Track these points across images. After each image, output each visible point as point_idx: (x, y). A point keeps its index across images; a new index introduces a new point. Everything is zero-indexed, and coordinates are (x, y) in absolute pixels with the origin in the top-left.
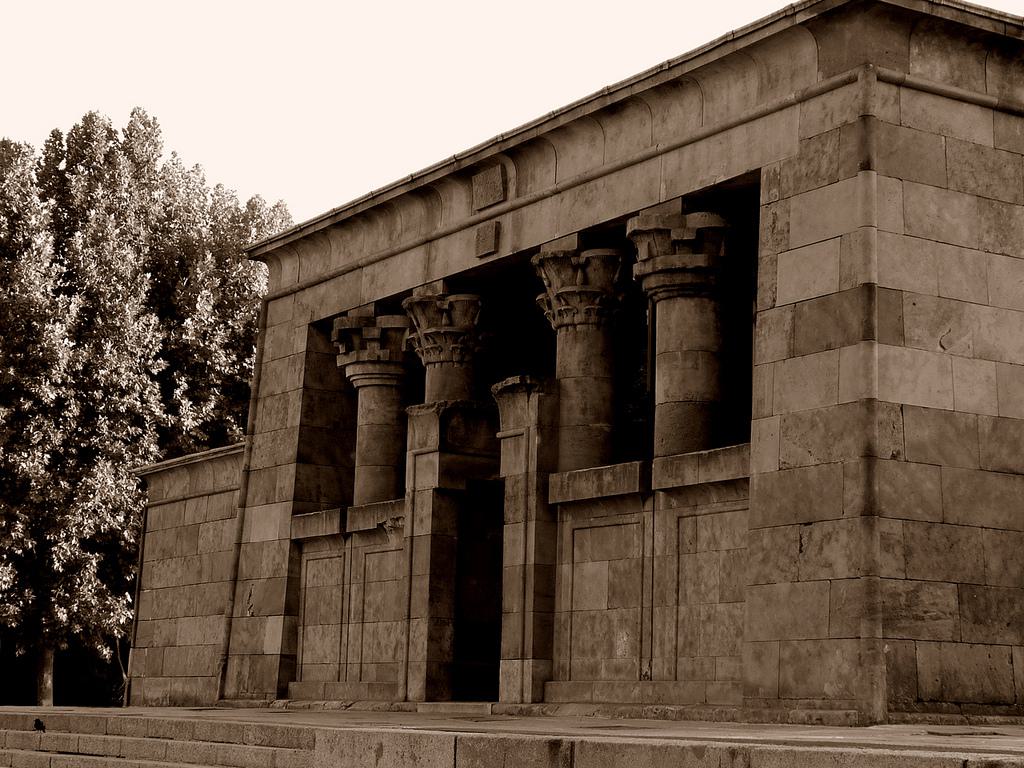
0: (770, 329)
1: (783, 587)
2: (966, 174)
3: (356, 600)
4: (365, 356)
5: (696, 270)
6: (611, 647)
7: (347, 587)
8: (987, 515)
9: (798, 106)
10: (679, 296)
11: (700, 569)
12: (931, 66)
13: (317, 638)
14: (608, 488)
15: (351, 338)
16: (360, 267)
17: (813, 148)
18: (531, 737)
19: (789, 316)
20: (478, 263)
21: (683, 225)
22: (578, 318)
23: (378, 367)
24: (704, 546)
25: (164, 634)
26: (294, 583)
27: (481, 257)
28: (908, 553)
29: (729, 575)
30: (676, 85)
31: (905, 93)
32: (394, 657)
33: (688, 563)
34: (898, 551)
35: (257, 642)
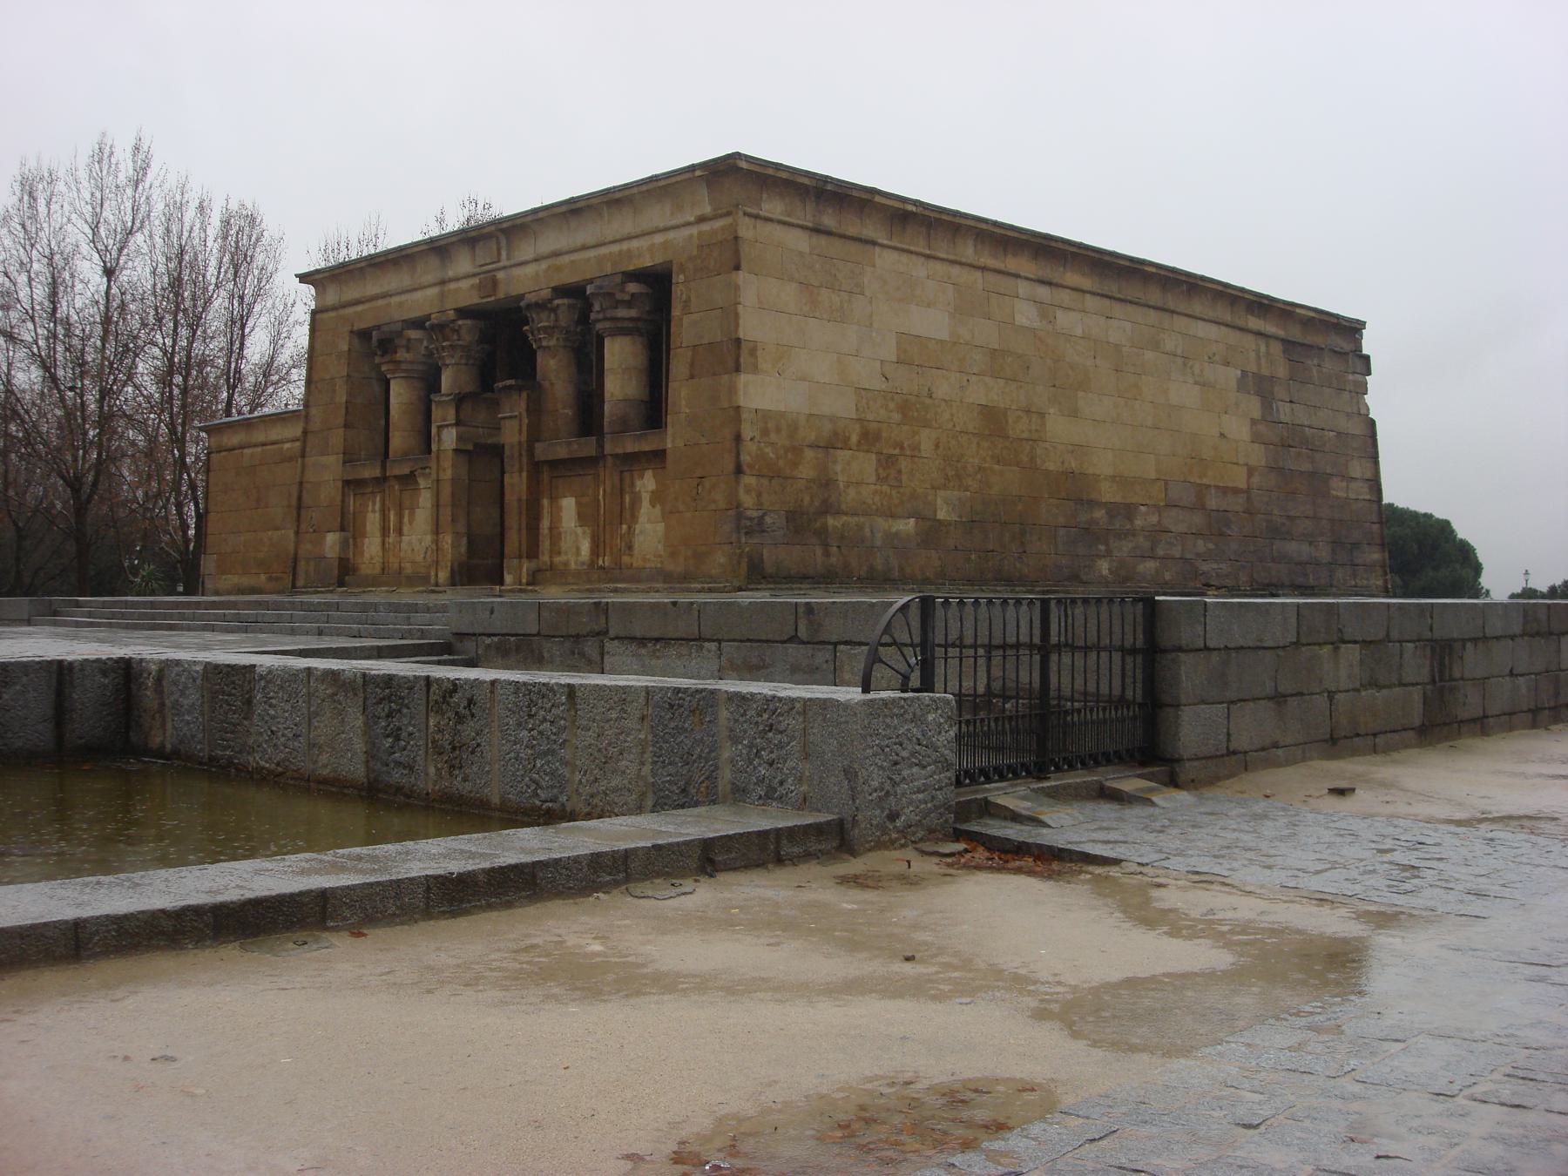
5: (631, 319)
6: (578, 549)
12: (773, 206)
19: (690, 353)
21: (623, 291)
28: (759, 495)
30: (618, 202)
31: (759, 223)
34: (754, 494)
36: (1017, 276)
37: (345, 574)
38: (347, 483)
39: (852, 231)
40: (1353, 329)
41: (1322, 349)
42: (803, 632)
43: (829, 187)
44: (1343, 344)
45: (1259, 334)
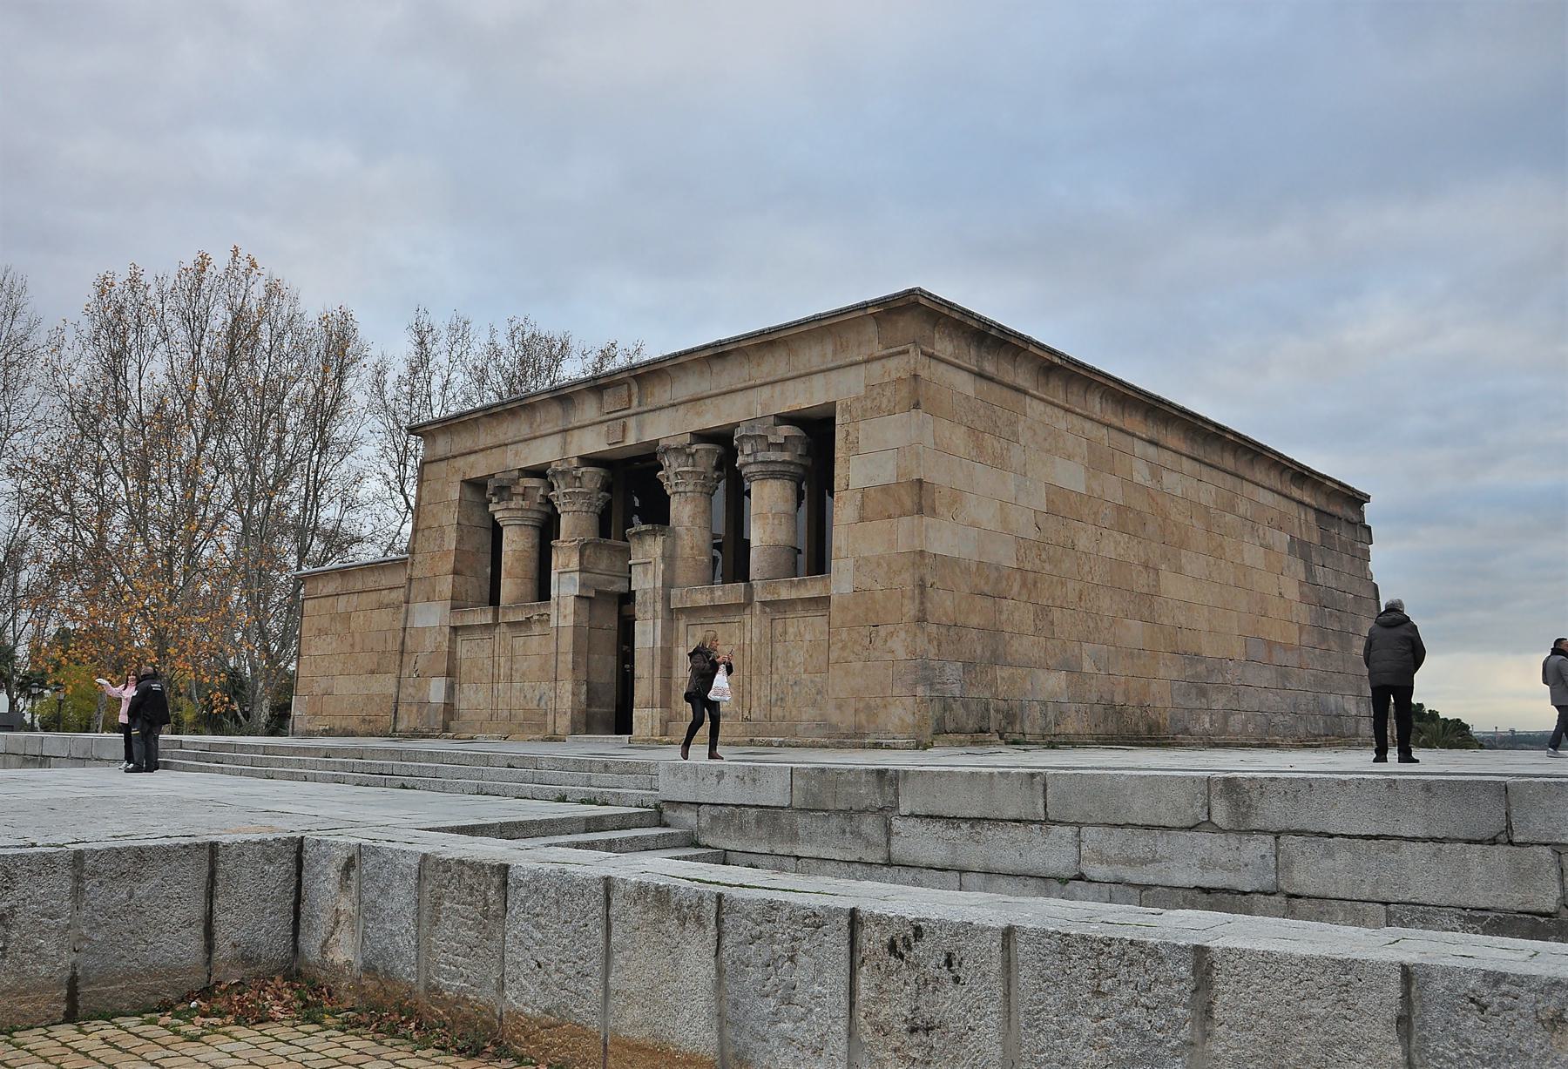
0: (845, 503)
1: (858, 665)
2: (962, 413)
3: (505, 667)
4: (512, 505)
5: (783, 462)
7: (496, 658)
8: (975, 620)
9: (864, 365)
10: (771, 478)
11: (788, 652)
13: (472, 692)
14: (720, 599)
15: (503, 491)
16: (507, 445)
17: (875, 392)
18: (1016, 770)
20: (608, 448)
22: (690, 488)
23: (520, 512)
24: (792, 638)
25: (322, 686)
26: (452, 654)
27: (610, 444)
29: (811, 656)
31: (933, 362)
32: (538, 706)
33: (779, 648)
34: (935, 643)
35: (423, 695)
36: (1134, 435)
37: (449, 720)
38: (455, 630)
39: (1008, 379)
40: (1357, 500)
41: (1340, 519)
42: (1220, 815)
43: (993, 332)
44: (1349, 513)
45: (1301, 503)
